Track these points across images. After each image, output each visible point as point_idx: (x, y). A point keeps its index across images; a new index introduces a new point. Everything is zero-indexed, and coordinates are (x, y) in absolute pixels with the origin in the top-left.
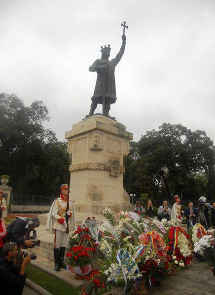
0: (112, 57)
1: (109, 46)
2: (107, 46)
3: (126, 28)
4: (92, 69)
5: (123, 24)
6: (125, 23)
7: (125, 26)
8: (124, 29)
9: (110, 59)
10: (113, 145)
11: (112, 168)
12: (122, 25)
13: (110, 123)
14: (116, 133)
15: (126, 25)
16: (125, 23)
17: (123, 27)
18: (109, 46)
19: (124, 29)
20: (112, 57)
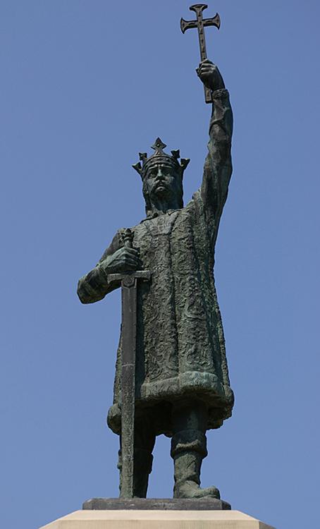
0: (193, 186)
1: (159, 144)
3: (209, 30)
4: (93, 289)
5: (192, 16)
8: (201, 33)
9: (187, 200)
12: (186, 26)
15: (207, 15)
17: (194, 32)
18: (159, 144)
19: (201, 33)
20: (193, 186)
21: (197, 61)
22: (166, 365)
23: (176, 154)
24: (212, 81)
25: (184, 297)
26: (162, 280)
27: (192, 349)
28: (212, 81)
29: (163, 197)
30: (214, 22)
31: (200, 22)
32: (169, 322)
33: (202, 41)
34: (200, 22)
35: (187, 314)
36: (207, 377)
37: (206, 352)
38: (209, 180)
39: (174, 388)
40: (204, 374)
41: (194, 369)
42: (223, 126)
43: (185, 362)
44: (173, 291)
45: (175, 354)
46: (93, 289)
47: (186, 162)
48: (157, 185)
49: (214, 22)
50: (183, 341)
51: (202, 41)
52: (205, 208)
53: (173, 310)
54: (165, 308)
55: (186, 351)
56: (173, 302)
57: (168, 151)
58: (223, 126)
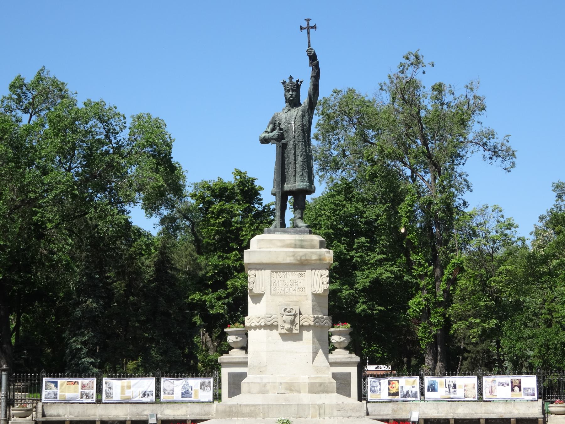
1: (291, 78)
2: (288, 81)
3: (312, 31)
5: (305, 24)
6: (308, 20)
7: (308, 28)
8: (309, 33)
10: (287, 280)
11: (280, 323)
13: (279, 244)
14: (289, 260)
15: (311, 24)
16: (308, 20)
17: (305, 31)
18: (291, 78)
19: (309, 33)
21: (307, 48)
22: (292, 179)
23: (298, 81)
24: (313, 58)
25: (299, 152)
26: (290, 146)
27: (301, 174)
28: (313, 58)
29: (293, 102)
30: (315, 27)
31: (308, 27)
32: (293, 162)
33: (309, 37)
34: (308, 27)
35: (300, 159)
36: (306, 185)
37: (306, 174)
38: (310, 98)
39: (294, 189)
40: (305, 184)
41: (302, 182)
42: (316, 77)
43: (298, 179)
44: (295, 149)
45: (295, 175)
46: (265, 141)
47: (301, 82)
48: (290, 97)
49: (315, 27)
50: (298, 170)
51: (309, 37)
52: (308, 109)
53: (295, 157)
54: (292, 156)
55: (299, 174)
56: (295, 154)
57: (294, 81)
58: (316, 77)
